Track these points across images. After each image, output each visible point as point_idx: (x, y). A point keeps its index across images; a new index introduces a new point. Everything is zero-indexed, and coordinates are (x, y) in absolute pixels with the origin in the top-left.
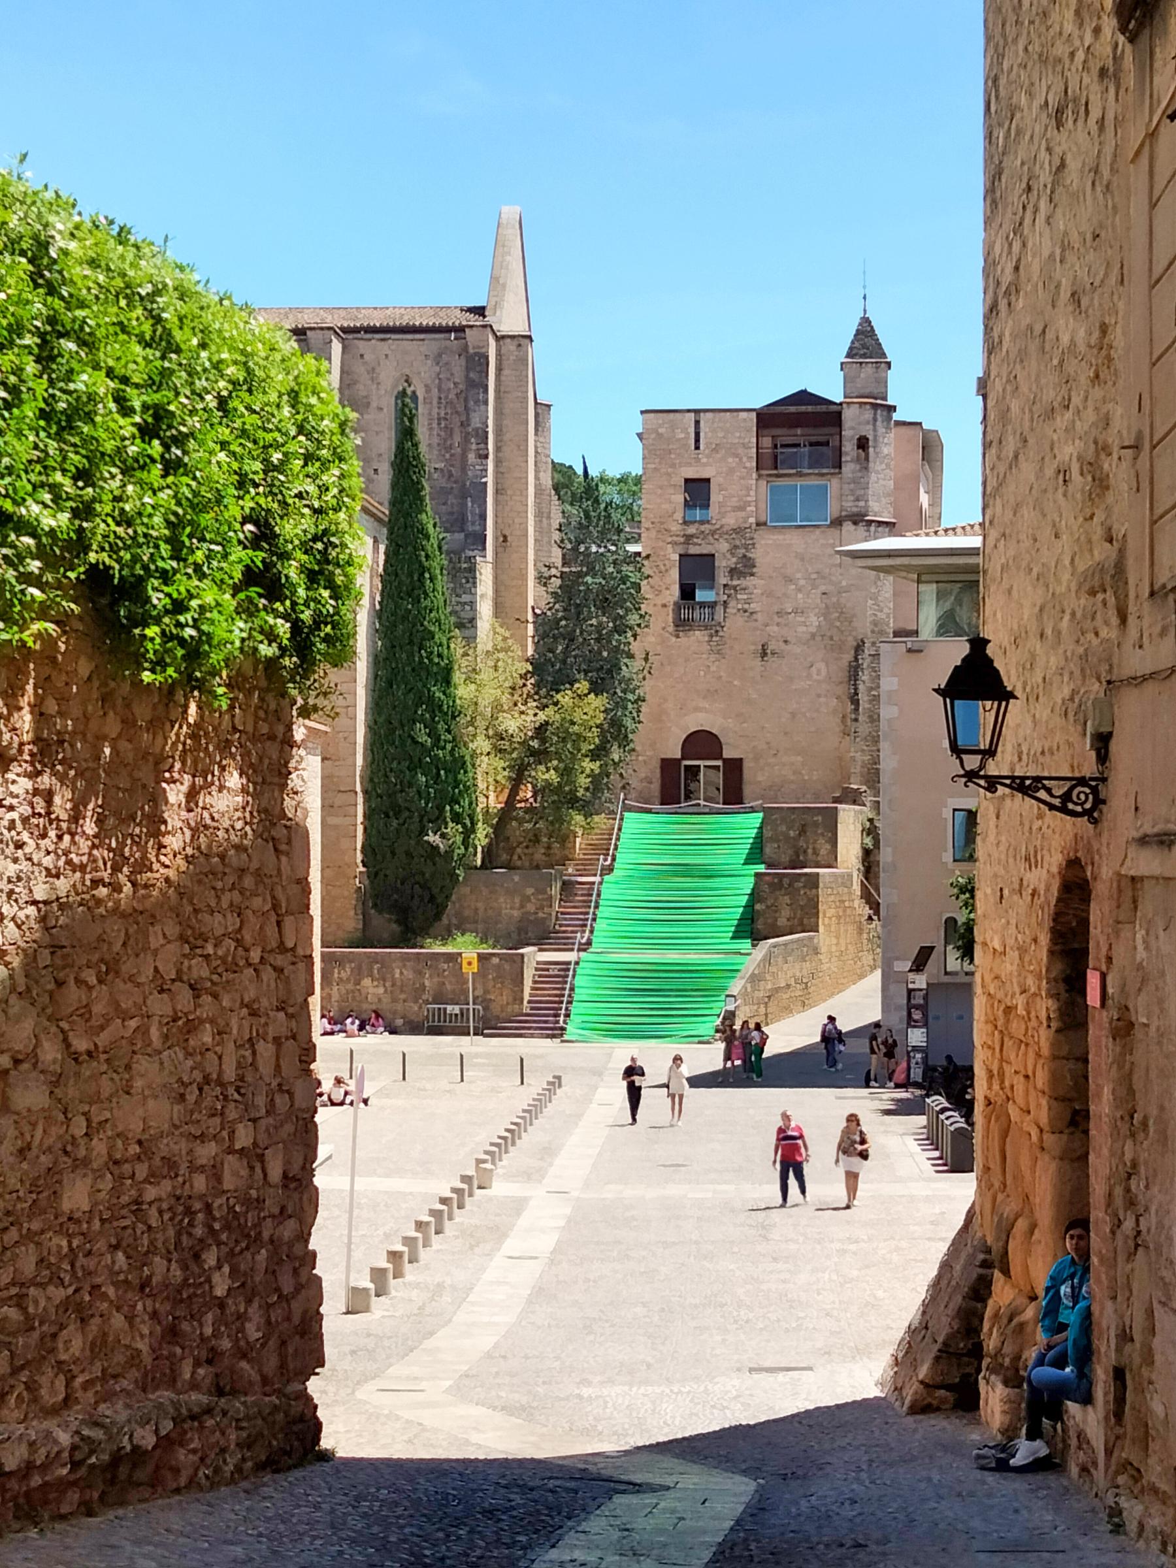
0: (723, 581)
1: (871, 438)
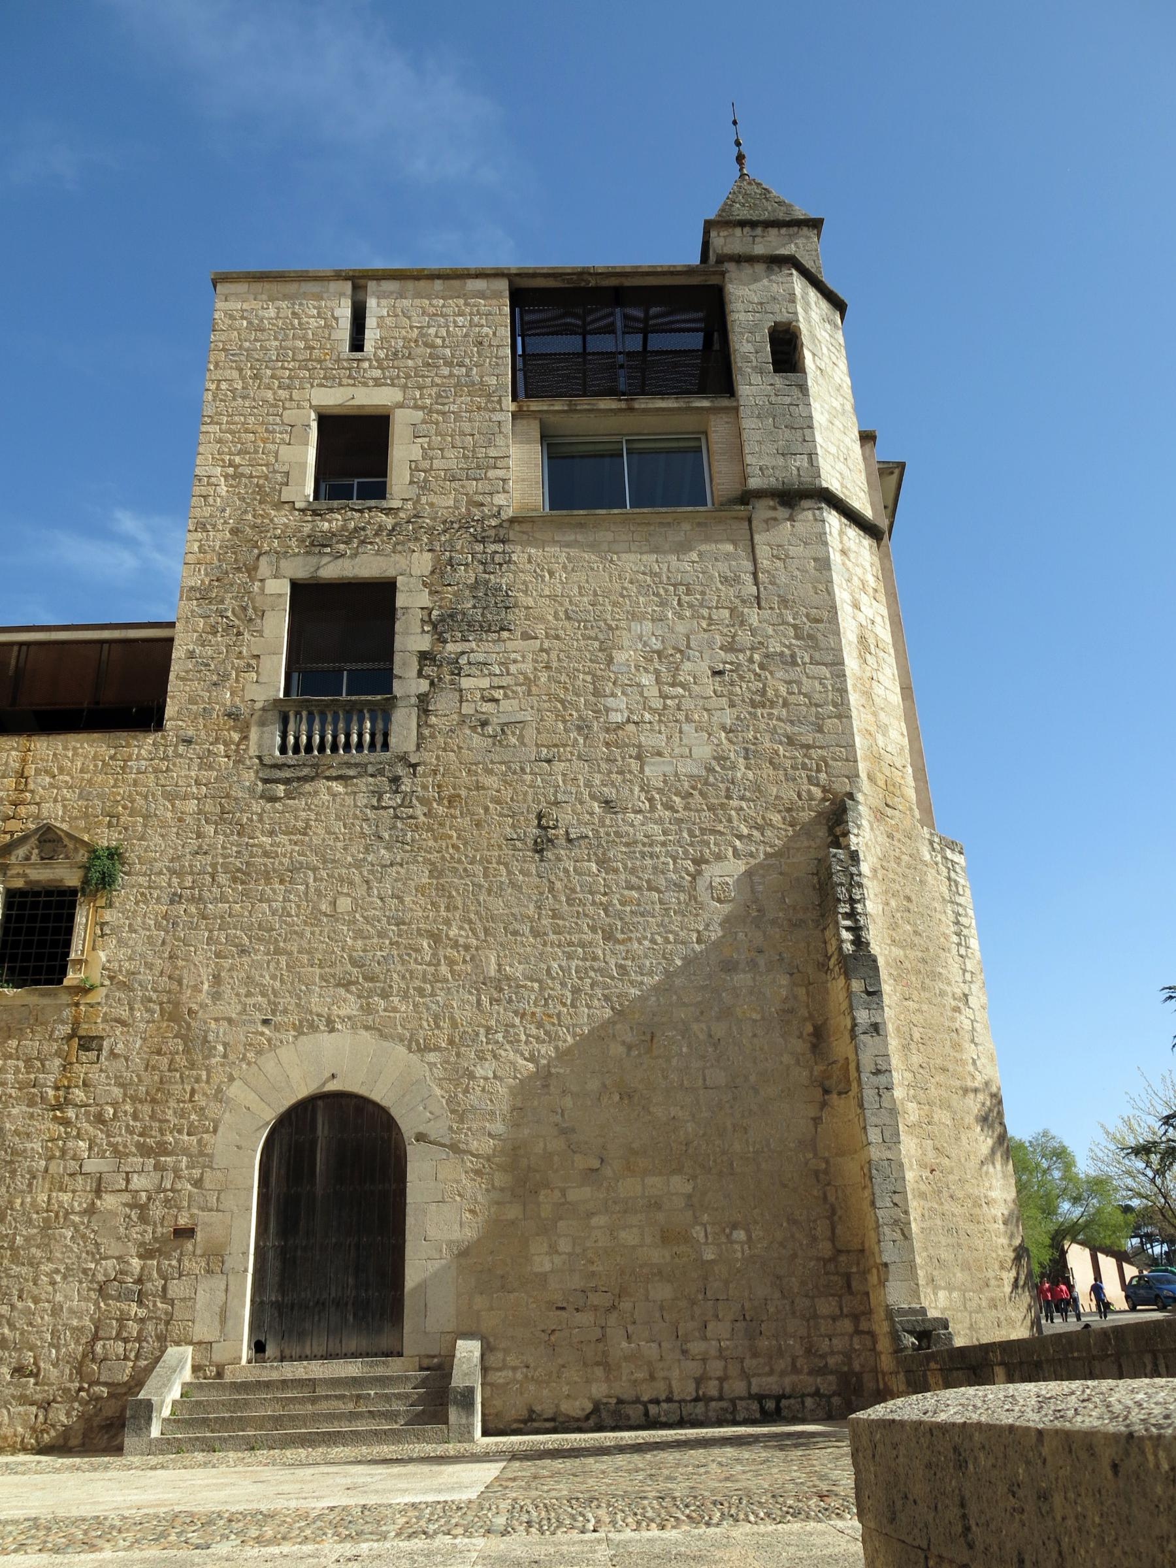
0: (424, 643)
1: (803, 326)
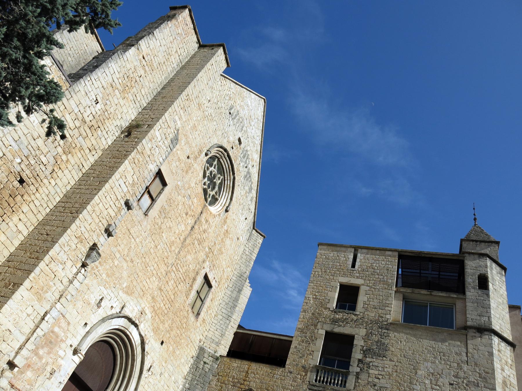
0: (360, 357)
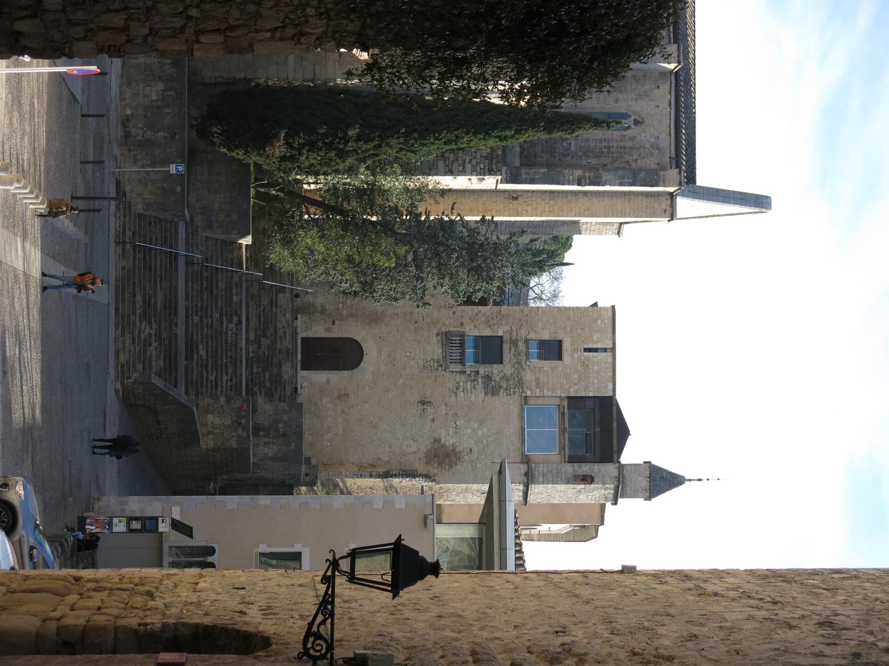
1: (592, 486)
